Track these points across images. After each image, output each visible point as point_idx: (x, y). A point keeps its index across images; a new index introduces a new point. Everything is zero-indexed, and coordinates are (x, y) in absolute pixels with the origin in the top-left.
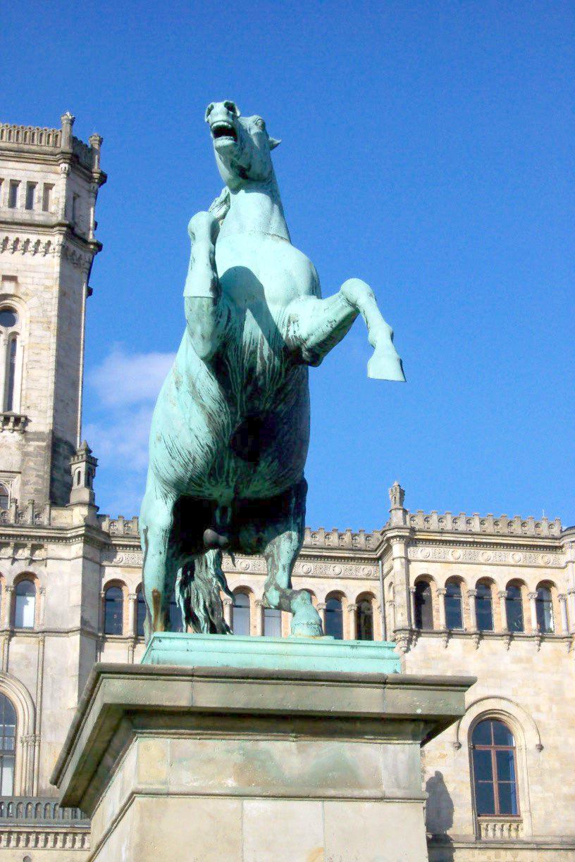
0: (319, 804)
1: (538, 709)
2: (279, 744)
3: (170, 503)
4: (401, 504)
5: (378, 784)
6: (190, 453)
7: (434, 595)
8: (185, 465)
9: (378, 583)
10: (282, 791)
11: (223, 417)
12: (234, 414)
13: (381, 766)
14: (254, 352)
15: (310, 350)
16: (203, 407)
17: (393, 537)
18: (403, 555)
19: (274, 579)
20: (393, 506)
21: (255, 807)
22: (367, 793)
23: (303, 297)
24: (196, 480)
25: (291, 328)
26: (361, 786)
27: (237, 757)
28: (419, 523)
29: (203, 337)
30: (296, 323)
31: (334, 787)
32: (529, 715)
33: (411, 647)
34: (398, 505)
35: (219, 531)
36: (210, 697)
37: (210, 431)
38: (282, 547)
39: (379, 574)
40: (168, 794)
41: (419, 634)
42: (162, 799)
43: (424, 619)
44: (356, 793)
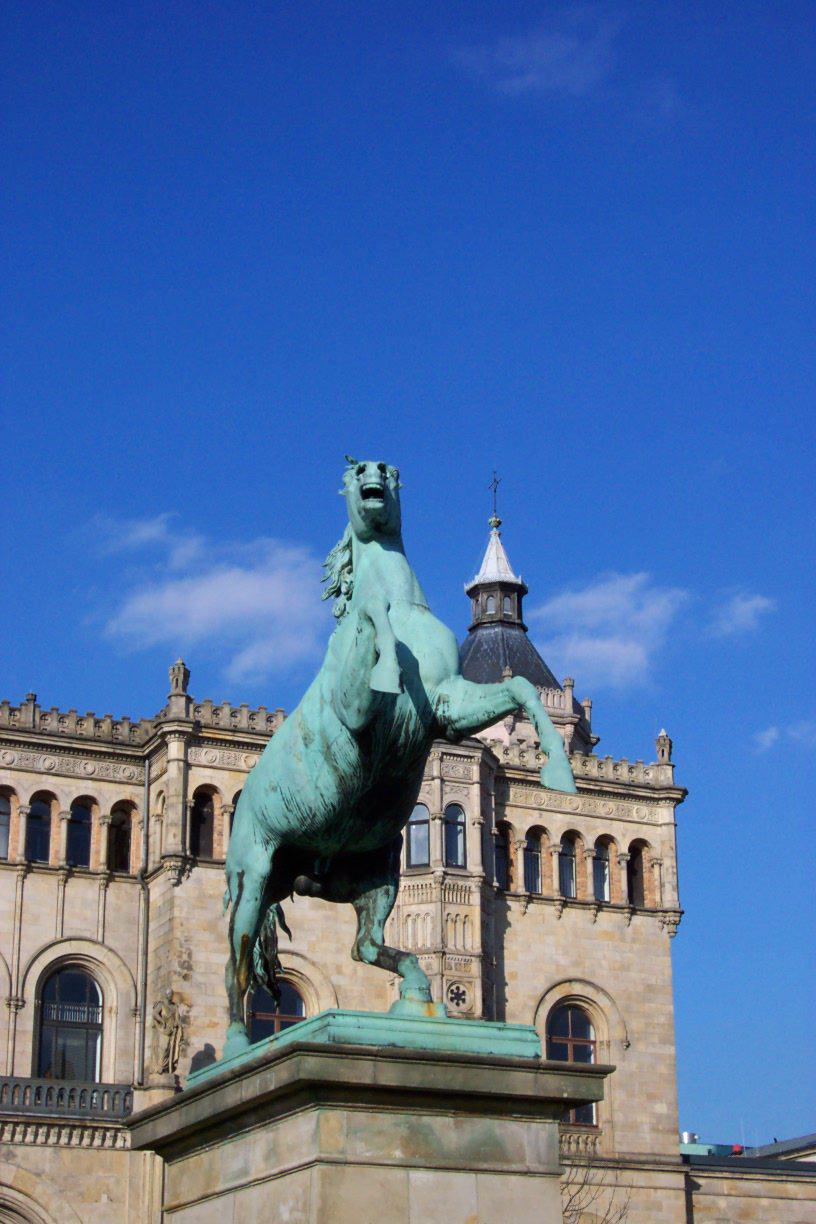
0: (473, 1176)
1: (339, 970)
2: (439, 1119)
3: (271, 850)
4: (184, 689)
5: (522, 1160)
6: (310, 809)
7: (217, 812)
8: (303, 820)
9: (142, 790)
10: (443, 1163)
11: (355, 781)
12: (366, 779)
13: (525, 1143)
14: (400, 726)
15: (456, 730)
16: (336, 769)
17: (170, 733)
18: (182, 757)
19: (369, 933)
20: (173, 691)
21: (420, 1177)
22: (514, 1167)
23: (453, 677)
24: (311, 834)
25: (441, 708)
26: (508, 1161)
27: (404, 1131)
28: (205, 716)
29: (359, 711)
31: (485, 1161)
32: (327, 978)
33: (183, 879)
34: (179, 690)
35: (313, 878)
36: (390, 1075)
37: (339, 793)
38: (379, 902)
39: (144, 778)
40: (346, 1163)
41: (194, 864)
42: (339, 1168)
43: (202, 843)
44: (505, 1167)
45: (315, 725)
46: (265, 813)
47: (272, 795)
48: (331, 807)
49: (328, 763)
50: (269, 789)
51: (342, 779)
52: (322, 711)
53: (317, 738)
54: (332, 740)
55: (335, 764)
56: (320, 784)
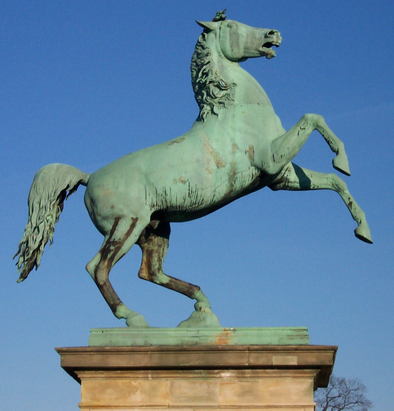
3: (153, 210)
6: (203, 200)
16: (232, 185)
25: (287, 173)
30: (289, 172)
37: (223, 197)
45: (228, 158)
46: (168, 192)
47: (180, 184)
48: (213, 202)
49: (229, 181)
50: (178, 181)
51: (231, 191)
52: (234, 152)
53: (228, 166)
54: (238, 171)
55: (233, 183)
56: (217, 190)
